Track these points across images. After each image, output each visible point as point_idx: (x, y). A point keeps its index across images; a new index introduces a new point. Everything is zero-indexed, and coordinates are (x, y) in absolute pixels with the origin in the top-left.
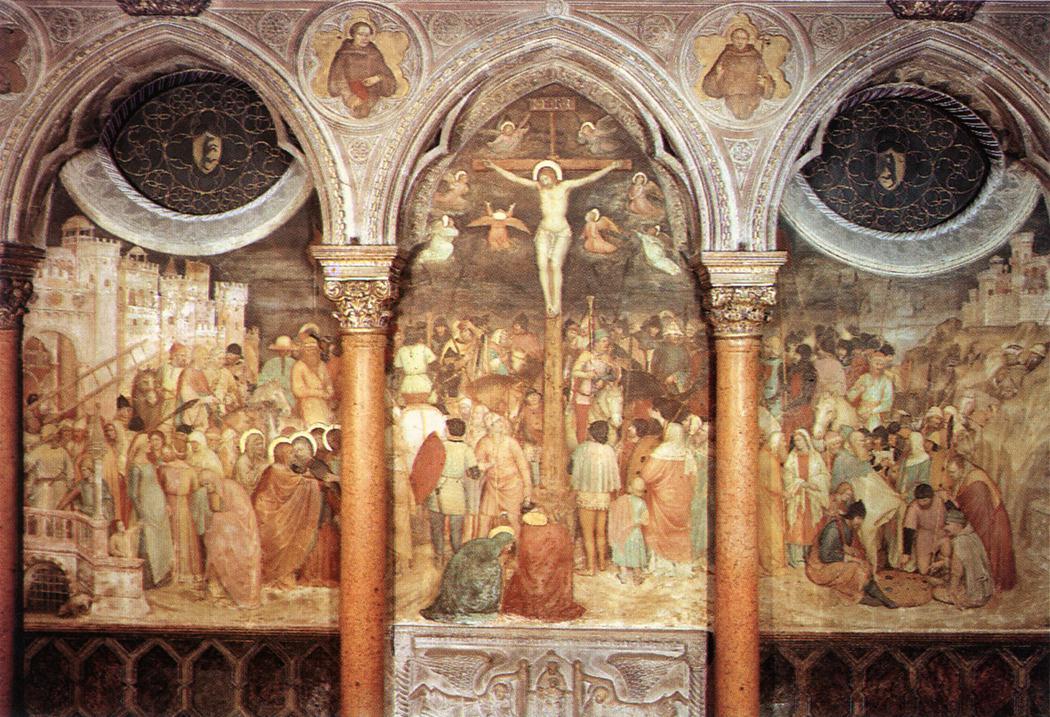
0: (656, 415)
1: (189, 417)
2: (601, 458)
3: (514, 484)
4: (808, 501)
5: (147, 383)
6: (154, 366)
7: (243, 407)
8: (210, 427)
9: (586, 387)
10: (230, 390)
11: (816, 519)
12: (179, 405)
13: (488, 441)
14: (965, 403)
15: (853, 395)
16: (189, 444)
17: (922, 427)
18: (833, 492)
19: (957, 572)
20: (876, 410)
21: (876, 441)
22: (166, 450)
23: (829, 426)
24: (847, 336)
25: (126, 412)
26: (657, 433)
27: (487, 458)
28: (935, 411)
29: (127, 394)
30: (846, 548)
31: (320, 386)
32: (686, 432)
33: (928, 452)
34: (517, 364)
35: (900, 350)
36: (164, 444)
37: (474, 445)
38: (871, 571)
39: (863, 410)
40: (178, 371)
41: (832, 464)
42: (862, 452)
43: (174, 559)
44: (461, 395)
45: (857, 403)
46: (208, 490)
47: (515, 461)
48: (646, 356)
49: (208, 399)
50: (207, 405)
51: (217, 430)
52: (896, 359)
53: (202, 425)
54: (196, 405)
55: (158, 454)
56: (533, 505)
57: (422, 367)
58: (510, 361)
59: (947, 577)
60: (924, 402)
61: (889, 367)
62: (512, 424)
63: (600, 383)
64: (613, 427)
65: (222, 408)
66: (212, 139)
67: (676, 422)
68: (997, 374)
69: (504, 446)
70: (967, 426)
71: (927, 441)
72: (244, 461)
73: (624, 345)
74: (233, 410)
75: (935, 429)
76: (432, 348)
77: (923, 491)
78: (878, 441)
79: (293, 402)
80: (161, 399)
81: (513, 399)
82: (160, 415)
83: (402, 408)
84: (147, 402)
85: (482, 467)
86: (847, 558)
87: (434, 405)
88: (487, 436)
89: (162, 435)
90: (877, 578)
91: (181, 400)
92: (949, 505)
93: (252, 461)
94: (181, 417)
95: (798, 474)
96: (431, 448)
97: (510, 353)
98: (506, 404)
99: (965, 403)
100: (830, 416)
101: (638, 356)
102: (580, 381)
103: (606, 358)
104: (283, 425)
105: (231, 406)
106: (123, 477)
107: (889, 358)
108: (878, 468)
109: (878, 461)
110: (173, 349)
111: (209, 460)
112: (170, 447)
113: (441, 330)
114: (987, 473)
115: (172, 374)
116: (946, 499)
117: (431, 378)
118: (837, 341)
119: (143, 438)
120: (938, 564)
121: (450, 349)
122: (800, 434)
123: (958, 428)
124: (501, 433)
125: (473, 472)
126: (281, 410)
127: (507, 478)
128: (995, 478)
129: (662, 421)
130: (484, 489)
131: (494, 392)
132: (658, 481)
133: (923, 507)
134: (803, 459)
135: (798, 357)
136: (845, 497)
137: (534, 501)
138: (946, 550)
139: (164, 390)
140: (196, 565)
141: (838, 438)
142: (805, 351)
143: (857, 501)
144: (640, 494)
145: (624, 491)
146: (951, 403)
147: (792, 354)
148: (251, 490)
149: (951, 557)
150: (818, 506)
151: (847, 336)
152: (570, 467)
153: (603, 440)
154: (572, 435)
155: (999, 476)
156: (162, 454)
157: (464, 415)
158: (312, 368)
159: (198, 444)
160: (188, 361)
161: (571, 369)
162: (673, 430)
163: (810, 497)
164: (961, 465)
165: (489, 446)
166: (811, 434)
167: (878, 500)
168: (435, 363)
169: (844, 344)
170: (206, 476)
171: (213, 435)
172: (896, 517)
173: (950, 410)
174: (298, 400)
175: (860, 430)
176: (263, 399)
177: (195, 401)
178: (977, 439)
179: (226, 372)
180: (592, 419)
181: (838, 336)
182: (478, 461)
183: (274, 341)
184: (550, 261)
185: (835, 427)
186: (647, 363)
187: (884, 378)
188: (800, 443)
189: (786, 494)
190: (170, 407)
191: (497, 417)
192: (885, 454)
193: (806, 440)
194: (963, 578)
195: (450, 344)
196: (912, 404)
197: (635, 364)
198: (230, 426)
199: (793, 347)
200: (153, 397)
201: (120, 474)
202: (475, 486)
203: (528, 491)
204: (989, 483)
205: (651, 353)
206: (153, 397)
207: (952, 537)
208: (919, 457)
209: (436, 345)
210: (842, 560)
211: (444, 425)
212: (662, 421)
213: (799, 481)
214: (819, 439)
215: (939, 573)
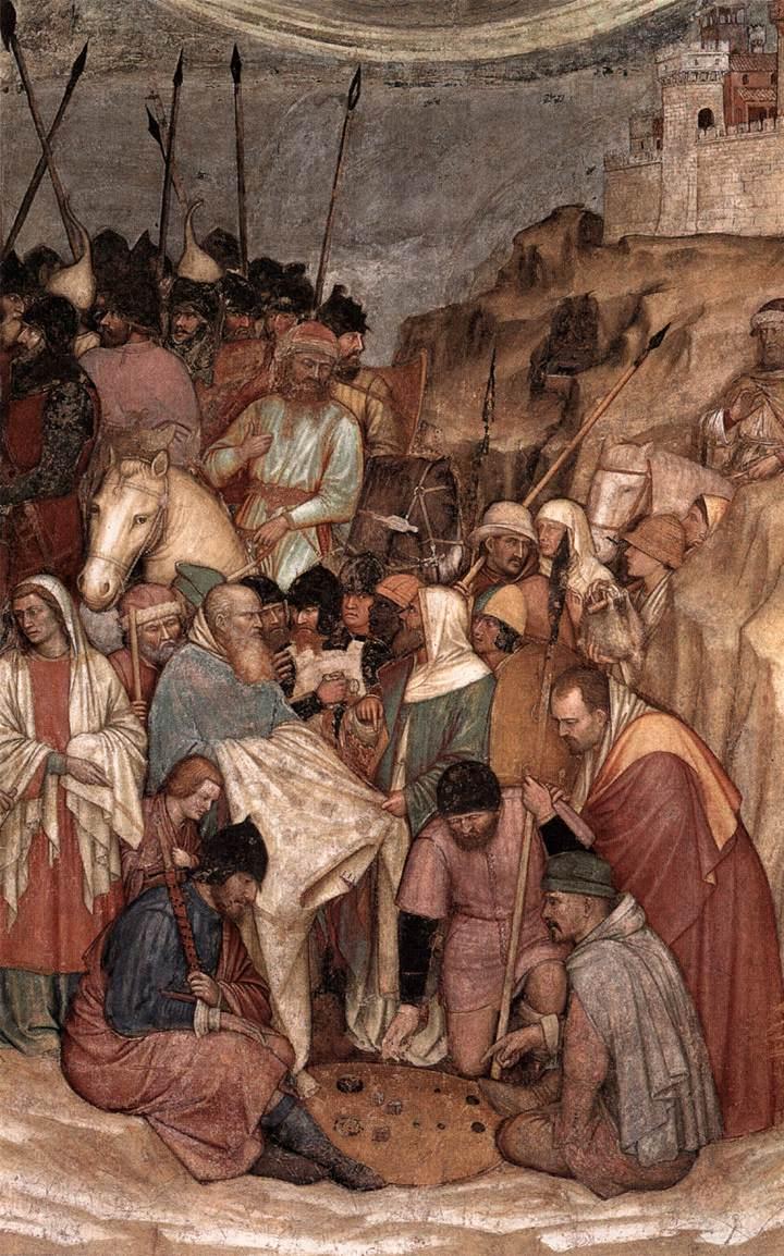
4: (69, 823)
11: (100, 878)
14: (612, 498)
15: (226, 461)
17: (462, 571)
18: (154, 789)
19: (585, 1062)
21: (301, 618)
23: (137, 570)
24: (202, 268)
28: (509, 516)
30: (202, 984)
33: (481, 655)
41: (149, 696)
42: (252, 658)
45: (235, 493)
52: (377, 350)
59: (551, 1084)
61: (349, 371)
68: (724, 398)
70: (619, 567)
71: (475, 617)
75: (510, 578)
78: (308, 617)
90: (308, 1084)
92: (554, 836)
95: (30, 730)
99: (612, 498)
100: (141, 533)
108: (308, 708)
109: (306, 683)
116: (546, 815)
118: (166, 284)
120: (519, 1040)
122: (42, 593)
123: (587, 575)
128: (717, 747)
133: (466, 843)
135: (34, 339)
136: (194, 806)
138: (547, 981)
141: (171, 607)
142: (55, 315)
143: (239, 819)
146: (561, 490)
149: (564, 1014)
150: (102, 836)
151: (202, 268)
163: (71, 803)
164: (598, 701)
169: (189, 291)
172: (377, 867)
173: (558, 512)
175: (245, 582)
178: (653, 611)
181: (170, 268)
185: (163, 567)
188: (40, 625)
192: (334, 661)
193: (57, 613)
194: (607, 1089)
196: (425, 492)
207: (572, 944)
210: (185, 1021)
214: (104, 608)
215: (524, 1068)
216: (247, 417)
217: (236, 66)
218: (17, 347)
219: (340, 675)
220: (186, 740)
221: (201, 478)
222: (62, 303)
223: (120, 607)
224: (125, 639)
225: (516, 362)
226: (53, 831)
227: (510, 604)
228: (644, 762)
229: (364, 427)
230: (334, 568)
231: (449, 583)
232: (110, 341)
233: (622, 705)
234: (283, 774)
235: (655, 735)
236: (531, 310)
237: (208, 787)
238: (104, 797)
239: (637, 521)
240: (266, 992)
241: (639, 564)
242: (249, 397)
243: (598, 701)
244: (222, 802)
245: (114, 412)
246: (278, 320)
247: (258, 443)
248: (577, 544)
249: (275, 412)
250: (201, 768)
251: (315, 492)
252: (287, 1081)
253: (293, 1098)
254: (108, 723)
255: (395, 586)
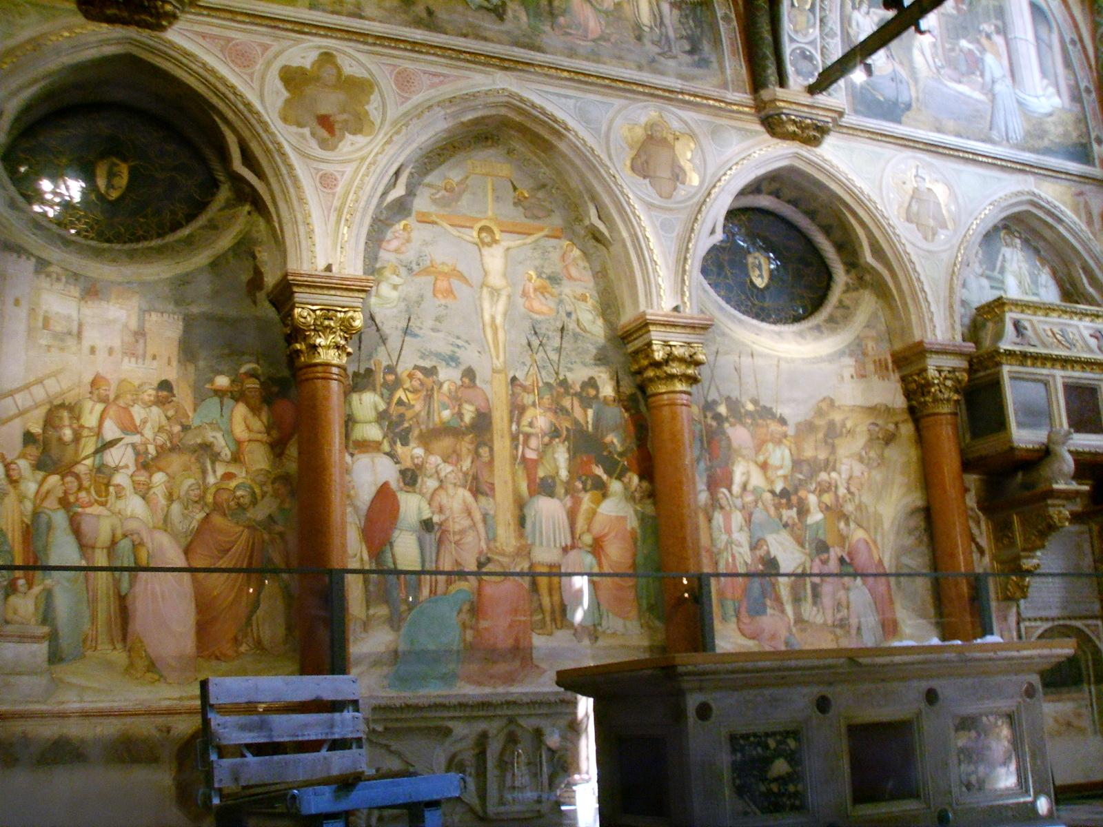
0: (599, 471)
1: (113, 457)
2: (549, 510)
3: (470, 538)
4: (733, 557)
5: (61, 419)
6: (70, 399)
7: (174, 449)
8: (138, 469)
9: (534, 443)
10: (161, 429)
12: (99, 445)
13: (442, 493)
15: (761, 458)
16: (111, 489)
18: (753, 548)
19: (854, 622)
20: (780, 473)
22: (83, 494)
23: (744, 487)
24: (750, 407)
25: (33, 451)
26: (601, 489)
27: (441, 510)
28: (823, 476)
29: (36, 429)
31: (263, 429)
32: (626, 487)
33: (822, 511)
34: (468, 418)
35: (792, 422)
36: (80, 488)
37: (428, 495)
38: (789, 623)
39: (770, 473)
40: (99, 407)
41: (750, 521)
42: (772, 511)
43: (87, 626)
44: (412, 445)
45: (764, 466)
46: (133, 542)
47: (469, 513)
48: (586, 416)
49: (136, 439)
50: (134, 446)
51: (146, 474)
52: (791, 431)
53: (126, 467)
54: (121, 443)
55: (72, 499)
56: (489, 560)
57: (372, 415)
58: (460, 415)
60: (816, 467)
62: (466, 474)
63: (546, 439)
64: (562, 481)
65: (152, 450)
66: (117, 165)
67: (616, 478)
69: (458, 498)
70: (848, 489)
72: (176, 508)
73: (567, 402)
74: (162, 451)
76: (382, 396)
77: (822, 547)
78: (784, 501)
79: (233, 448)
80: (77, 438)
81: (464, 450)
82: (77, 452)
83: (352, 455)
84: (60, 439)
85: (436, 519)
86: (769, 611)
87: (387, 454)
88: (441, 487)
89: (77, 477)
90: (794, 630)
91: (103, 439)
93: (186, 508)
94: (102, 457)
96: (385, 497)
97: (460, 405)
98: (459, 458)
100: (744, 478)
101: (578, 413)
102: (528, 436)
103: (550, 415)
104: (221, 470)
105: (161, 447)
106: (28, 526)
107: (784, 428)
108: (786, 526)
109: (785, 518)
110: (94, 383)
111: (134, 505)
112: (88, 492)
113: (391, 378)
114: (866, 530)
115: (92, 409)
116: (839, 555)
117: (382, 428)
119: (54, 479)
120: (839, 616)
121: (400, 399)
123: (842, 491)
124: (455, 485)
125: (427, 525)
126: (219, 454)
127: (462, 532)
129: (605, 477)
130: (440, 542)
131: (446, 443)
132: (605, 536)
134: (727, 518)
137: (489, 555)
139: (82, 427)
140: (117, 632)
142: (718, 417)
144: (589, 549)
145: (573, 547)
146: (834, 469)
147: (709, 421)
148: (184, 542)
149: (848, 608)
151: (750, 407)
152: (521, 521)
153: (551, 494)
154: (524, 487)
155: (876, 532)
156: (77, 500)
157: (416, 465)
158: (255, 410)
159: (124, 488)
160: (112, 397)
161: (518, 424)
162: (615, 486)
164: (847, 524)
165: (443, 498)
166: (730, 491)
167: (789, 556)
168: (386, 411)
169: (748, 413)
170: (132, 525)
171: (142, 477)
173: (834, 475)
174: (239, 443)
176: (199, 441)
177: (122, 439)
178: (857, 501)
179: (155, 409)
180: (541, 473)
181: (743, 407)
182: (433, 513)
183: (211, 381)
184: (493, 318)
185: (750, 487)
186: (587, 422)
187: (783, 447)
188: (723, 502)
189: (715, 550)
190: (89, 446)
191: (449, 468)
195: (400, 394)
196: (805, 468)
197: (576, 422)
198: (160, 470)
199: (709, 415)
200: (68, 434)
201: (23, 522)
202: (430, 539)
203: (483, 544)
204: (869, 541)
205: (590, 412)
206: (68, 434)
208: (816, 517)
209: (385, 391)
210: (764, 613)
211: (397, 475)
212: (605, 477)
213: (724, 537)
216: (764, 447)
217: (752, 355)
218: (711, 426)
219: (791, 517)
220: (759, 534)
221: (756, 463)
222: (720, 415)
223: (741, 497)
224: (744, 507)
225: (820, 435)
226: (730, 560)
227: (828, 498)
228: (858, 541)
229: (790, 450)
230: (789, 488)
231: (813, 492)
232: (732, 425)
233: (852, 525)
234: (781, 544)
235: (859, 534)
236: (821, 422)
237: (765, 547)
238: (741, 550)
239: (850, 478)
240: (782, 604)
241: (853, 489)
242: (764, 442)
243: (847, 524)
244: (768, 552)
245: (735, 444)
246: (769, 422)
247: (767, 454)
248: (839, 483)
249: (770, 446)
250: (762, 542)
251: (781, 467)
252: (789, 630)
253: (791, 634)
254: (741, 529)
255: (802, 493)
